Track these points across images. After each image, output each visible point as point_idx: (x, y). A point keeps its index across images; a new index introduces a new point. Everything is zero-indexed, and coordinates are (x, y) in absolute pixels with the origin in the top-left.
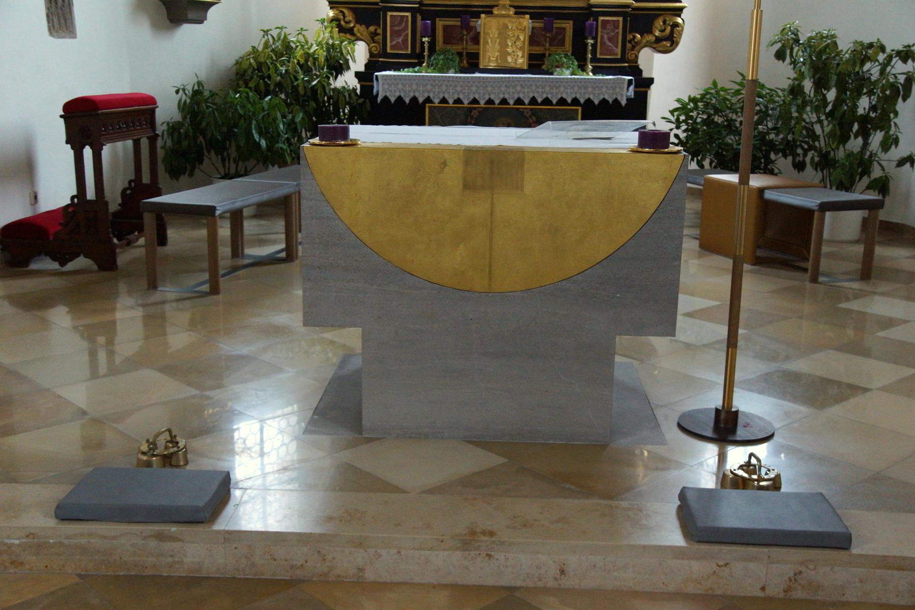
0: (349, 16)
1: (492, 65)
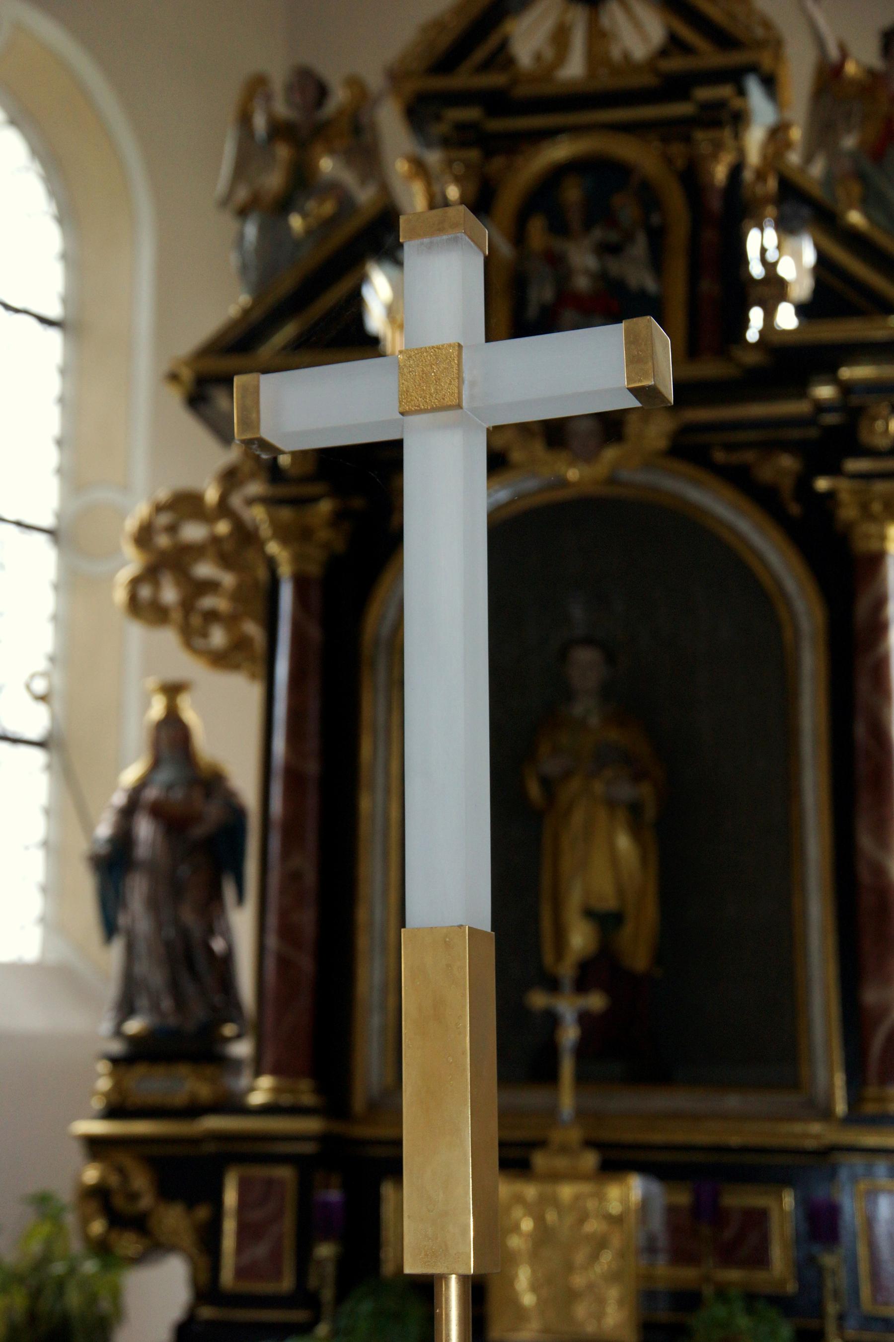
0: (141, 1181)
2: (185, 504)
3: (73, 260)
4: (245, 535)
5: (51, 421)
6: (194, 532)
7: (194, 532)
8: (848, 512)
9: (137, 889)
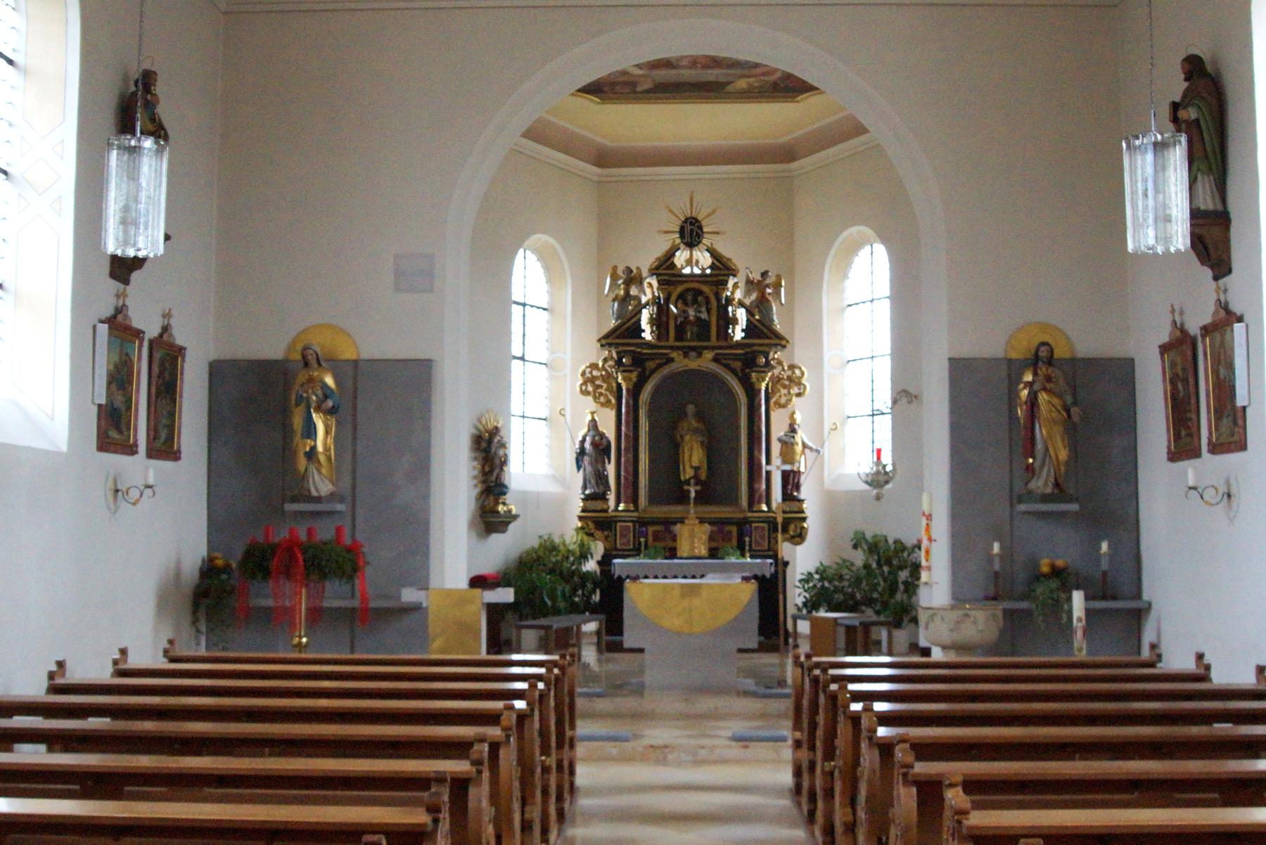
0: (591, 525)
1: (685, 555)
2: (594, 366)
3: (551, 293)
4: (609, 375)
5: (545, 335)
6: (595, 373)
7: (595, 373)
9: (586, 459)
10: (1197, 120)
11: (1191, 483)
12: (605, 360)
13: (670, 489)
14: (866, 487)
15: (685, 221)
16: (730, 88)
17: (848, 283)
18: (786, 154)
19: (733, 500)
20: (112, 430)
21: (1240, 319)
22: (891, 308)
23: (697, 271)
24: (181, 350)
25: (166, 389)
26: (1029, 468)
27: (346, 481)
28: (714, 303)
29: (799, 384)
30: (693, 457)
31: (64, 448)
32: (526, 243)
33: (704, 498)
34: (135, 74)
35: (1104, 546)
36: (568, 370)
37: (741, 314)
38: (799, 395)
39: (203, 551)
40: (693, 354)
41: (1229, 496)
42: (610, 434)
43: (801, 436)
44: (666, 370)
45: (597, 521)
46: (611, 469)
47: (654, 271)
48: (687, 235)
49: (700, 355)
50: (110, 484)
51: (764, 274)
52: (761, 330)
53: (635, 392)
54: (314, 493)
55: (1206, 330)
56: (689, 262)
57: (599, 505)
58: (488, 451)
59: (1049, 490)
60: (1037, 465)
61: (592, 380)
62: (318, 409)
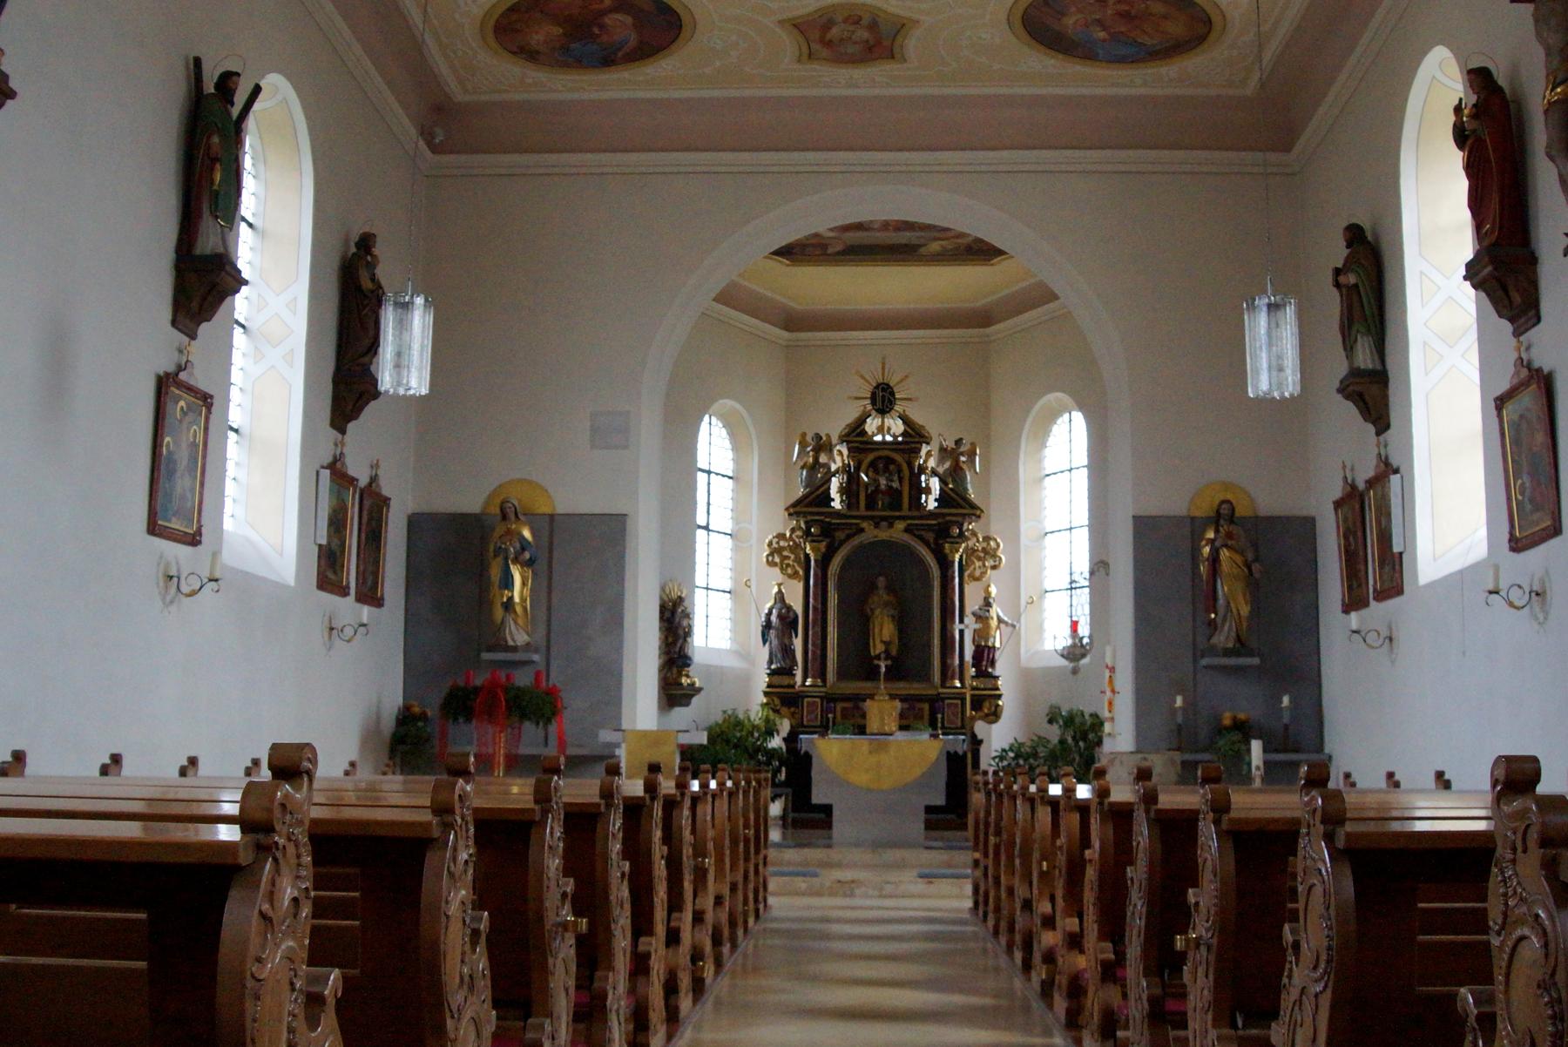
0: (777, 701)
2: (781, 536)
4: (797, 545)
8: (947, 551)
10: (1356, 286)
11: (1354, 627)
12: (793, 530)
13: (859, 664)
14: (1064, 662)
15: (877, 387)
16: (923, 250)
17: (1047, 452)
18: (982, 318)
19: (926, 677)
20: (328, 570)
21: (1396, 471)
22: (1090, 478)
23: (889, 438)
24: (386, 501)
25: (373, 537)
26: (1212, 625)
27: (542, 631)
28: (906, 472)
29: (994, 556)
30: (884, 631)
31: (291, 581)
32: (715, 407)
33: (895, 674)
34: (355, 237)
35: (1286, 700)
36: (754, 541)
37: (935, 484)
38: (994, 567)
39: (400, 701)
40: (884, 524)
41: (1391, 639)
42: (798, 608)
43: (996, 610)
44: (856, 541)
45: (782, 696)
46: (798, 644)
47: (844, 439)
48: (879, 400)
49: (891, 525)
50: (326, 623)
51: (958, 442)
52: (956, 502)
53: (824, 563)
54: (511, 643)
55: (1370, 483)
56: (881, 430)
57: (786, 680)
58: (674, 622)
59: (1230, 645)
60: (1219, 621)
61: (779, 551)
62: (516, 560)
